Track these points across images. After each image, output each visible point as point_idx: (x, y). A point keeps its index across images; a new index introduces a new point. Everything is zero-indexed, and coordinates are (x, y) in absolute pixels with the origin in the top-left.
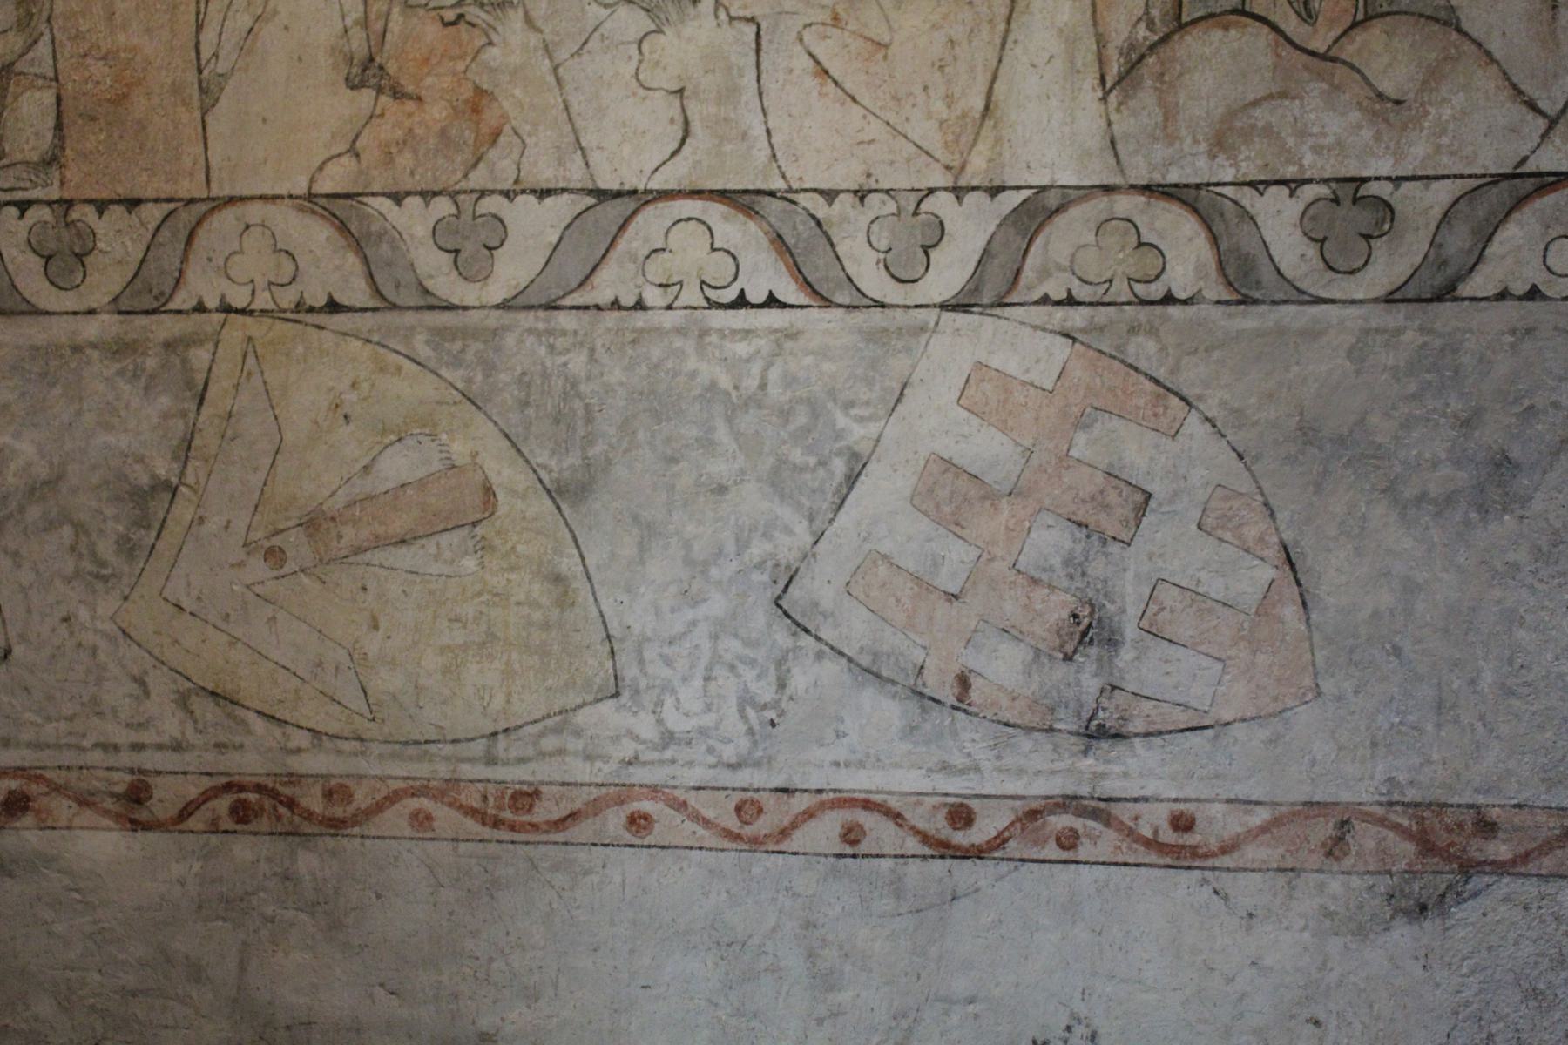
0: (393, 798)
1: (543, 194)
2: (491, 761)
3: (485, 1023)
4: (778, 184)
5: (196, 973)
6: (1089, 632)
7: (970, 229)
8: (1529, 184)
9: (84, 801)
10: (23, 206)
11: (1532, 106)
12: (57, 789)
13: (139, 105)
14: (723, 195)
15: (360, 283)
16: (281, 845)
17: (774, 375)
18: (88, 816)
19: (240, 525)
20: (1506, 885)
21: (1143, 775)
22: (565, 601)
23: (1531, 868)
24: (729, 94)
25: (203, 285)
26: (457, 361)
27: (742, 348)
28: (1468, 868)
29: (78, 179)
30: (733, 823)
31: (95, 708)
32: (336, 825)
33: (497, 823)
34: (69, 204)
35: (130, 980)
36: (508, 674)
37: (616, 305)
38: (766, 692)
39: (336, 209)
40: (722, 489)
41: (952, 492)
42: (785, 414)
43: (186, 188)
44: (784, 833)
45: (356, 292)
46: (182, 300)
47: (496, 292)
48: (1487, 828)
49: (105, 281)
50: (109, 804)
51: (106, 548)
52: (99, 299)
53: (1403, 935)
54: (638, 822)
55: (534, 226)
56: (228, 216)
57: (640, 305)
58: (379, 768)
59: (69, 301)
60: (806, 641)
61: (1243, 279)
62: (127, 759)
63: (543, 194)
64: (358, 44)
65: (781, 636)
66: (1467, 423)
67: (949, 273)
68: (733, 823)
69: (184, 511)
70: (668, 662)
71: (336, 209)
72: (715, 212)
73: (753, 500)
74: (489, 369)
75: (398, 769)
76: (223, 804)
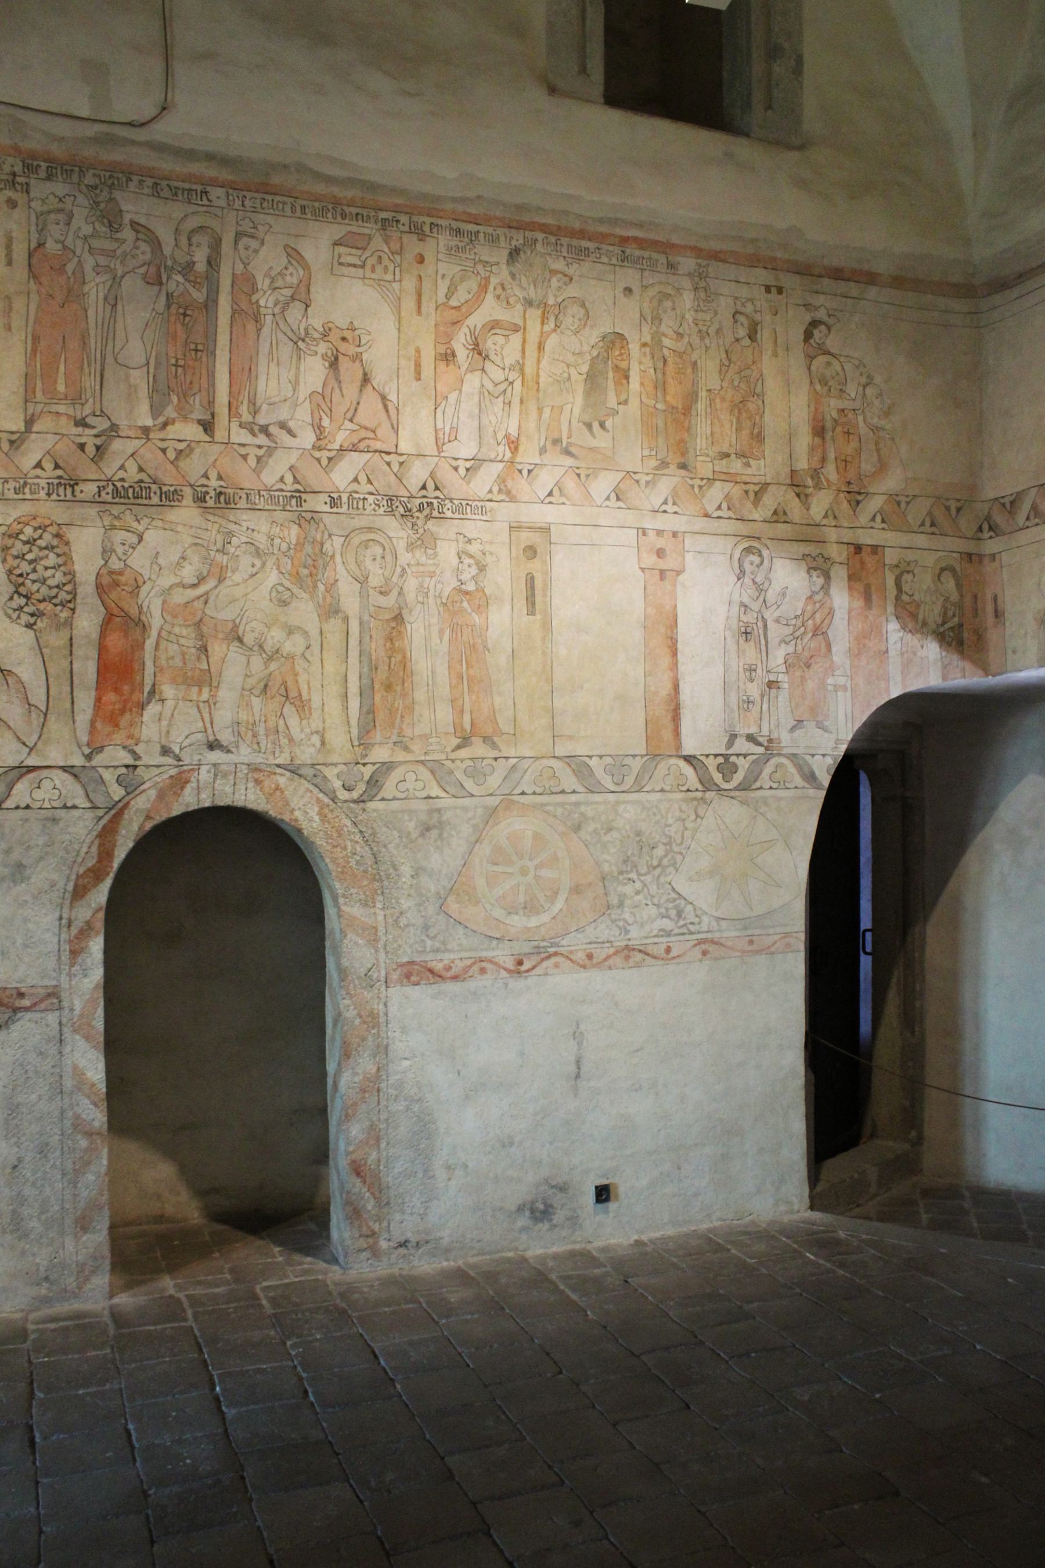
8: (25, 770)
11: (24, 744)
20: (29, 1015)
23: (37, 1008)
28: (16, 1010)
48: (21, 995)
66: (8, 852)
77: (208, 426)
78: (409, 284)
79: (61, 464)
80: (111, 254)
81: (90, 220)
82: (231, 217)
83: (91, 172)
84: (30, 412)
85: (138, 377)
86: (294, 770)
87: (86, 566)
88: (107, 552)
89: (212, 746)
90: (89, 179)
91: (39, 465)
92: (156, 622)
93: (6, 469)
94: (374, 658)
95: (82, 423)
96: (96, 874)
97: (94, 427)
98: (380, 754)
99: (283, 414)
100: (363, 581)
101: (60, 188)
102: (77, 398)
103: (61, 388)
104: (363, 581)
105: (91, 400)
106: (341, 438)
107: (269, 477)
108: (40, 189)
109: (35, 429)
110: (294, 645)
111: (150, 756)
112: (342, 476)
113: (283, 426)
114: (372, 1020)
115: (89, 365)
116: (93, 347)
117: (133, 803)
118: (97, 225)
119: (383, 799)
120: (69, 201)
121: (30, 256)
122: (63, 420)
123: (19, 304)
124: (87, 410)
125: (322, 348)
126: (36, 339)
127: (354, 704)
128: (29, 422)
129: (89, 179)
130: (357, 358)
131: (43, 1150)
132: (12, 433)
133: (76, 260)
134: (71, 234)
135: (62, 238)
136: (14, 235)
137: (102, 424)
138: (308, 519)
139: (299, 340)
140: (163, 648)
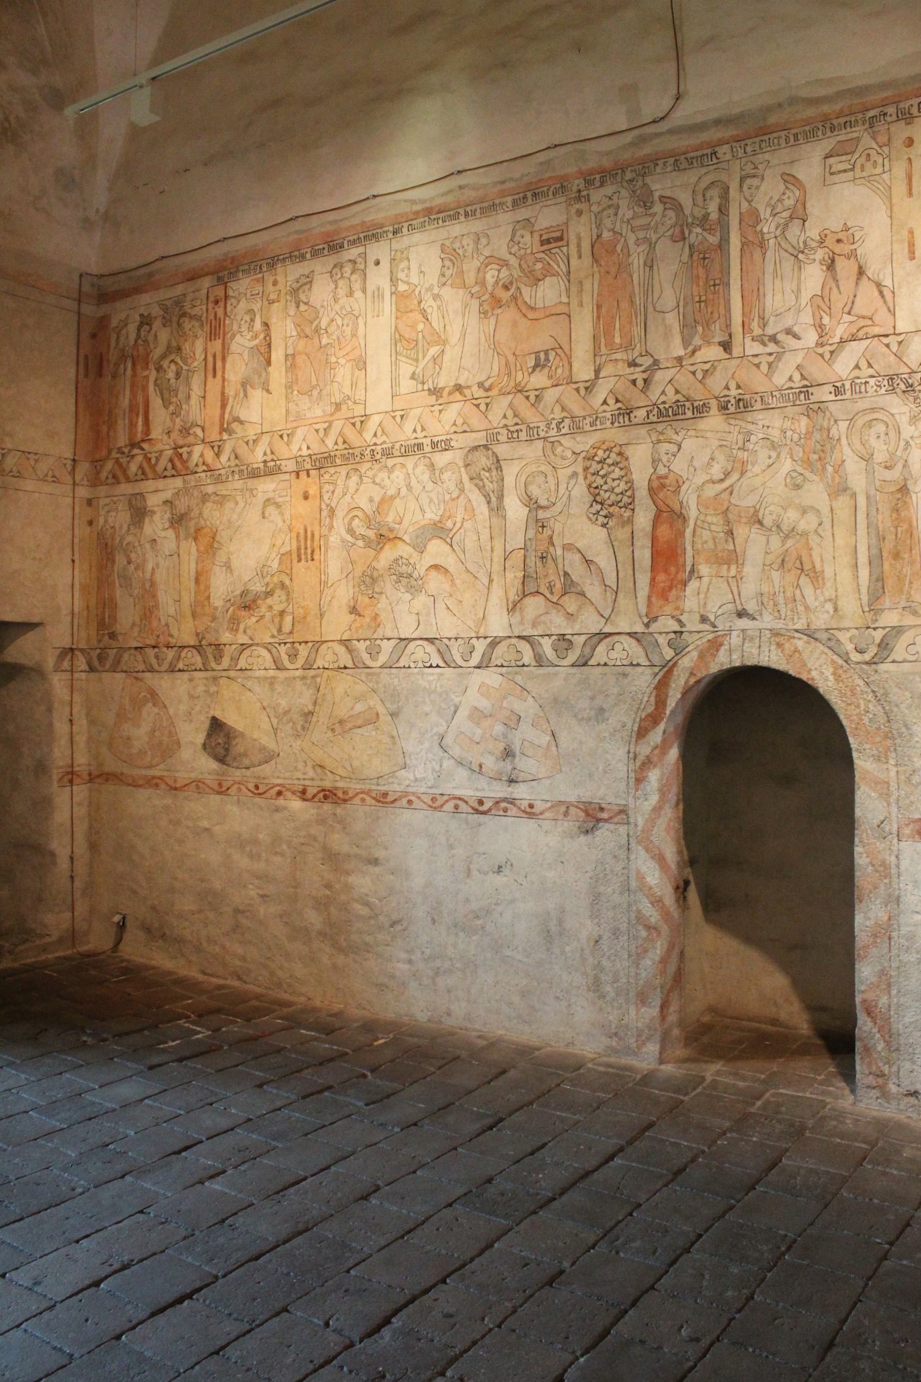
0: (357, 794)
1: (389, 639)
2: (378, 785)
3: (376, 856)
4: (438, 637)
5: (315, 839)
6: (508, 753)
7: (480, 646)
8: (603, 636)
9: (294, 793)
10: (285, 643)
11: (602, 616)
12: (288, 790)
13: (308, 619)
14: (427, 639)
15: (351, 662)
16: (334, 805)
17: (438, 685)
18: (294, 797)
19: (326, 723)
20: (607, 825)
21: (521, 792)
22: (394, 743)
23: (612, 821)
24: (428, 614)
25: (320, 663)
26: (371, 681)
27: (431, 678)
28: (599, 820)
29: (296, 637)
30: (430, 803)
31: (296, 769)
32: (345, 801)
33: (379, 801)
34: (294, 643)
35: (302, 840)
36: (381, 762)
37: (404, 667)
38: (438, 768)
39: (344, 642)
40: (427, 714)
41: (477, 715)
42: (441, 695)
43: (317, 639)
44: (442, 806)
45: (350, 664)
46: (315, 666)
47: (379, 664)
48: (602, 809)
49: (300, 661)
50: (298, 794)
51: (299, 728)
52: (299, 666)
53: (583, 839)
54: (410, 802)
55: (387, 646)
56: (324, 646)
57: (409, 667)
58: (356, 786)
59: (293, 666)
60: (446, 754)
61: (540, 661)
62: (302, 782)
63: (389, 639)
64: (352, 604)
65: (441, 753)
66: (593, 698)
67: (476, 659)
68: (430, 803)
69: (314, 719)
70: (416, 759)
71: (344, 642)
72: (425, 643)
73: (434, 717)
74: (377, 683)
75: (358, 786)
76: (321, 795)
77: (726, 346)
78: (899, 170)
79: (620, 398)
80: (646, 228)
81: (631, 206)
82: (736, 166)
83: (629, 169)
84: (598, 363)
85: (672, 319)
86: (810, 634)
87: (641, 475)
88: (655, 462)
89: (741, 614)
90: (629, 175)
91: (605, 402)
92: (693, 513)
93: (584, 409)
94: (881, 529)
95: (633, 364)
96: (654, 719)
97: (641, 365)
98: (890, 619)
99: (788, 322)
100: (867, 458)
101: (609, 190)
102: (628, 346)
103: (617, 340)
104: (867, 458)
105: (638, 345)
106: (840, 332)
107: (780, 379)
108: (597, 195)
109: (601, 376)
110: (807, 523)
111: (693, 623)
112: (843, 366)
113: (789, 332)
114: (884, 870)
115: (636, 318)
116: (638, 303)
117: (680, 662)
118: (635, 208)
119: (893, 662)
120: (615, 197)
121: (592, 247)
122: (620, 365)
123: (587, 285)
124: (636, 353)
125: (820, 254)
126: (599, 307)
127: (864, 573)
128: (597, 372)
129: (629, 175)
130: (853, 254)
131: (616, 932)
132: (587, 381)
133: (623, 239)
134: (618, 221)
135: (612, 227)
136: (582, 235)
137: (647, 362)
138: (815, 410)
139: (798, 254)
140: (700, 536)
